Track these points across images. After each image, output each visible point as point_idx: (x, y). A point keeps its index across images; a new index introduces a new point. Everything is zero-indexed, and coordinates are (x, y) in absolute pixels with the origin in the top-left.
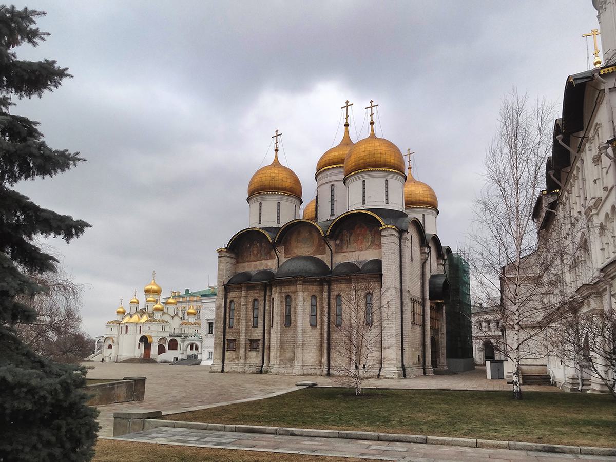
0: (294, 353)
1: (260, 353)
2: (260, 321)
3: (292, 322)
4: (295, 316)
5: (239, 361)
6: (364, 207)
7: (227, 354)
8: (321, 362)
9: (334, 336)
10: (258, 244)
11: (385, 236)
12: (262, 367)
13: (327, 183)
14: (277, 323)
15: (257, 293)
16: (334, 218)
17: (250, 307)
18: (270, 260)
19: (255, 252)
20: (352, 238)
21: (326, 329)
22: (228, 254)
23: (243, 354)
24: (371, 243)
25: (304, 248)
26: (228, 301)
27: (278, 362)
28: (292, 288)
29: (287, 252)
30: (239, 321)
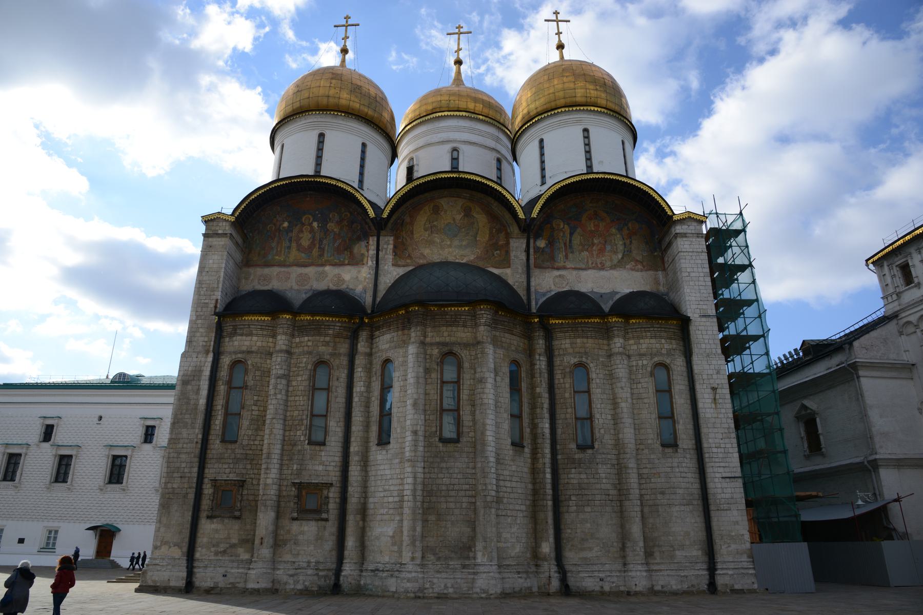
0: (472, 524)
1: (331, 528)
2: (335, 427)
3: (465, 430)
4: (473, 413)
5: (251, 551)
7: (207, 527)
8: (536, 556)
9: (573, 477)
10: (315, 224)
11: (684, 235)
12: (338, 571)
14: (415, 433)
15: (327, 344)
17: (301, 382)
18: (349, 267)
19: (305, 243)
20: (577, 240)
21: (549, 456)
23: (271, 528)
25: (450, 246)
26: (226, 361)
27: (418, 555)
28: (462, 334)
29: (400, 251)
30: (259, 423)
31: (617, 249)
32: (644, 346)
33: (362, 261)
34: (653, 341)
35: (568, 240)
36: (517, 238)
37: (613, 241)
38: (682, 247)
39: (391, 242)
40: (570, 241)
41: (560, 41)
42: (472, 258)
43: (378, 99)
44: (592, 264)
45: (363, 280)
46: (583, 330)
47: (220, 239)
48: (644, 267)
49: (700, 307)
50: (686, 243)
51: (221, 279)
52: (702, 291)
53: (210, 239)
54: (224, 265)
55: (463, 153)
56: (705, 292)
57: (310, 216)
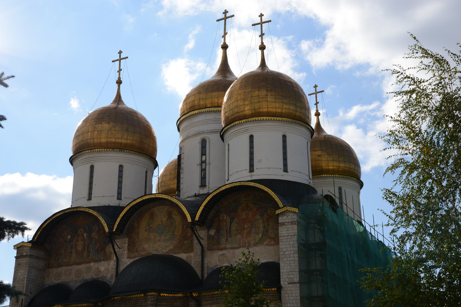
6: (251, 176)
10: (85, 235)
11: (283, 224)
13: (196, 135)
16: (205, 191)
19: (80, 248)
20: (234, 226)
22: (34, 253)
24: (263, 234)
29: (131, 247)
33: (111, 256)
35: (229, 227)
37: (257, 225)
38: (281, 233)
39: (127, 242)
40: (230, 228)
41: (262, 43)
42: (172, 248)
44: (243, 243)
45: (111, 270)
46: (216, 299)
47: (24, 259)
48: (275, 243)
49: (289, 276)
50: (284, 229)
51: (25, 285)
52: (292, 265)
53: (19, 260)
54: (26, 276)
55: (209, 142)
56: (294, 265)
57: (82, 230)
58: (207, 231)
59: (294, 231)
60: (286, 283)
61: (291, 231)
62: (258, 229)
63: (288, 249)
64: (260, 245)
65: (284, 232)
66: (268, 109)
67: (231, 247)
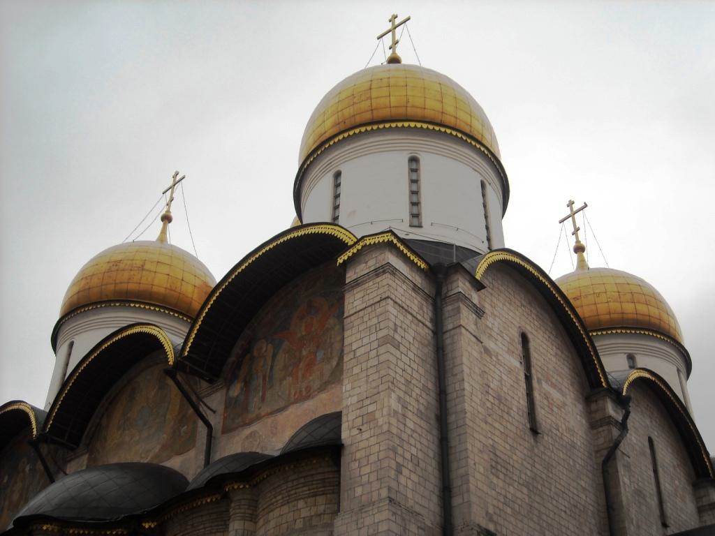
10: (27, 468)
31: (331, 354)
32: (272, 524)
34: (285, 509)
35: (269, 370)
36: (210, 395)
37: (328, 340)
39: (85, 462)
42: (157, 450)
43: (147, 267)
49: (364, 411)
58: (224, 391)
59: (380, 291)
60: (355, 432)
61: (375, 294)
62: (329, 350)
63: (366, 341)
64: (333, 386)
65: (356, 303)
66: (372, 113)
67: (269, 411)
